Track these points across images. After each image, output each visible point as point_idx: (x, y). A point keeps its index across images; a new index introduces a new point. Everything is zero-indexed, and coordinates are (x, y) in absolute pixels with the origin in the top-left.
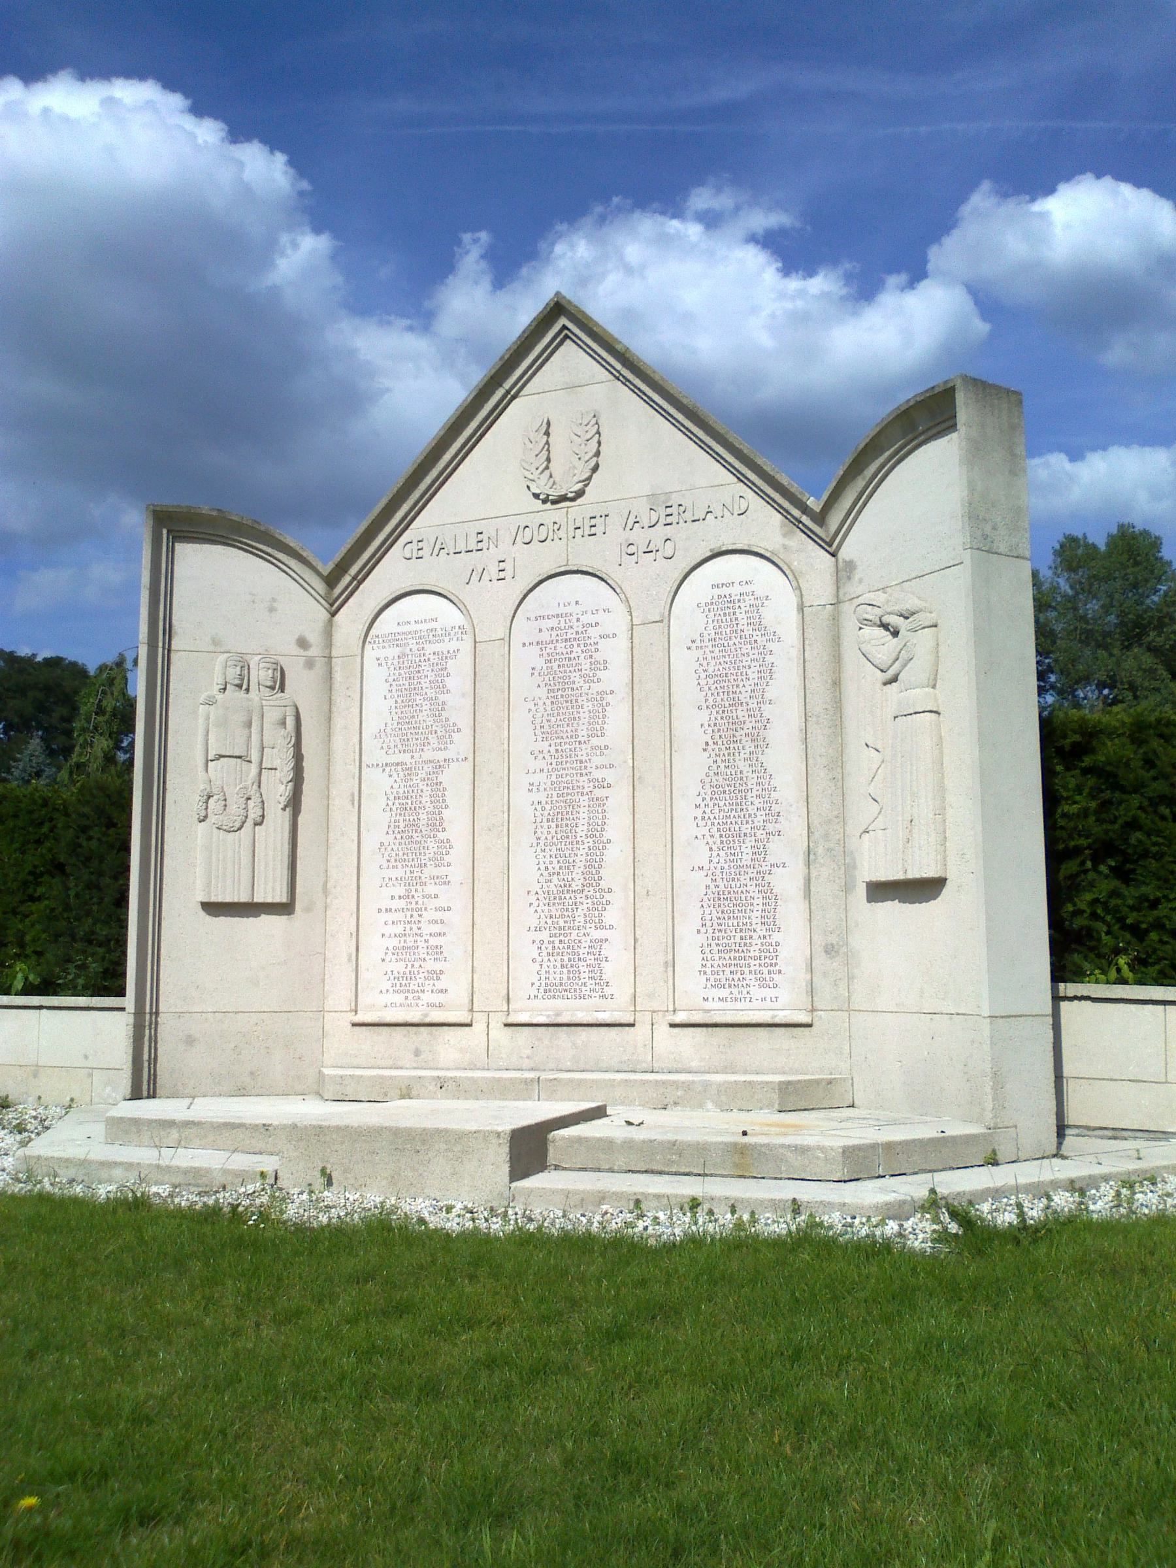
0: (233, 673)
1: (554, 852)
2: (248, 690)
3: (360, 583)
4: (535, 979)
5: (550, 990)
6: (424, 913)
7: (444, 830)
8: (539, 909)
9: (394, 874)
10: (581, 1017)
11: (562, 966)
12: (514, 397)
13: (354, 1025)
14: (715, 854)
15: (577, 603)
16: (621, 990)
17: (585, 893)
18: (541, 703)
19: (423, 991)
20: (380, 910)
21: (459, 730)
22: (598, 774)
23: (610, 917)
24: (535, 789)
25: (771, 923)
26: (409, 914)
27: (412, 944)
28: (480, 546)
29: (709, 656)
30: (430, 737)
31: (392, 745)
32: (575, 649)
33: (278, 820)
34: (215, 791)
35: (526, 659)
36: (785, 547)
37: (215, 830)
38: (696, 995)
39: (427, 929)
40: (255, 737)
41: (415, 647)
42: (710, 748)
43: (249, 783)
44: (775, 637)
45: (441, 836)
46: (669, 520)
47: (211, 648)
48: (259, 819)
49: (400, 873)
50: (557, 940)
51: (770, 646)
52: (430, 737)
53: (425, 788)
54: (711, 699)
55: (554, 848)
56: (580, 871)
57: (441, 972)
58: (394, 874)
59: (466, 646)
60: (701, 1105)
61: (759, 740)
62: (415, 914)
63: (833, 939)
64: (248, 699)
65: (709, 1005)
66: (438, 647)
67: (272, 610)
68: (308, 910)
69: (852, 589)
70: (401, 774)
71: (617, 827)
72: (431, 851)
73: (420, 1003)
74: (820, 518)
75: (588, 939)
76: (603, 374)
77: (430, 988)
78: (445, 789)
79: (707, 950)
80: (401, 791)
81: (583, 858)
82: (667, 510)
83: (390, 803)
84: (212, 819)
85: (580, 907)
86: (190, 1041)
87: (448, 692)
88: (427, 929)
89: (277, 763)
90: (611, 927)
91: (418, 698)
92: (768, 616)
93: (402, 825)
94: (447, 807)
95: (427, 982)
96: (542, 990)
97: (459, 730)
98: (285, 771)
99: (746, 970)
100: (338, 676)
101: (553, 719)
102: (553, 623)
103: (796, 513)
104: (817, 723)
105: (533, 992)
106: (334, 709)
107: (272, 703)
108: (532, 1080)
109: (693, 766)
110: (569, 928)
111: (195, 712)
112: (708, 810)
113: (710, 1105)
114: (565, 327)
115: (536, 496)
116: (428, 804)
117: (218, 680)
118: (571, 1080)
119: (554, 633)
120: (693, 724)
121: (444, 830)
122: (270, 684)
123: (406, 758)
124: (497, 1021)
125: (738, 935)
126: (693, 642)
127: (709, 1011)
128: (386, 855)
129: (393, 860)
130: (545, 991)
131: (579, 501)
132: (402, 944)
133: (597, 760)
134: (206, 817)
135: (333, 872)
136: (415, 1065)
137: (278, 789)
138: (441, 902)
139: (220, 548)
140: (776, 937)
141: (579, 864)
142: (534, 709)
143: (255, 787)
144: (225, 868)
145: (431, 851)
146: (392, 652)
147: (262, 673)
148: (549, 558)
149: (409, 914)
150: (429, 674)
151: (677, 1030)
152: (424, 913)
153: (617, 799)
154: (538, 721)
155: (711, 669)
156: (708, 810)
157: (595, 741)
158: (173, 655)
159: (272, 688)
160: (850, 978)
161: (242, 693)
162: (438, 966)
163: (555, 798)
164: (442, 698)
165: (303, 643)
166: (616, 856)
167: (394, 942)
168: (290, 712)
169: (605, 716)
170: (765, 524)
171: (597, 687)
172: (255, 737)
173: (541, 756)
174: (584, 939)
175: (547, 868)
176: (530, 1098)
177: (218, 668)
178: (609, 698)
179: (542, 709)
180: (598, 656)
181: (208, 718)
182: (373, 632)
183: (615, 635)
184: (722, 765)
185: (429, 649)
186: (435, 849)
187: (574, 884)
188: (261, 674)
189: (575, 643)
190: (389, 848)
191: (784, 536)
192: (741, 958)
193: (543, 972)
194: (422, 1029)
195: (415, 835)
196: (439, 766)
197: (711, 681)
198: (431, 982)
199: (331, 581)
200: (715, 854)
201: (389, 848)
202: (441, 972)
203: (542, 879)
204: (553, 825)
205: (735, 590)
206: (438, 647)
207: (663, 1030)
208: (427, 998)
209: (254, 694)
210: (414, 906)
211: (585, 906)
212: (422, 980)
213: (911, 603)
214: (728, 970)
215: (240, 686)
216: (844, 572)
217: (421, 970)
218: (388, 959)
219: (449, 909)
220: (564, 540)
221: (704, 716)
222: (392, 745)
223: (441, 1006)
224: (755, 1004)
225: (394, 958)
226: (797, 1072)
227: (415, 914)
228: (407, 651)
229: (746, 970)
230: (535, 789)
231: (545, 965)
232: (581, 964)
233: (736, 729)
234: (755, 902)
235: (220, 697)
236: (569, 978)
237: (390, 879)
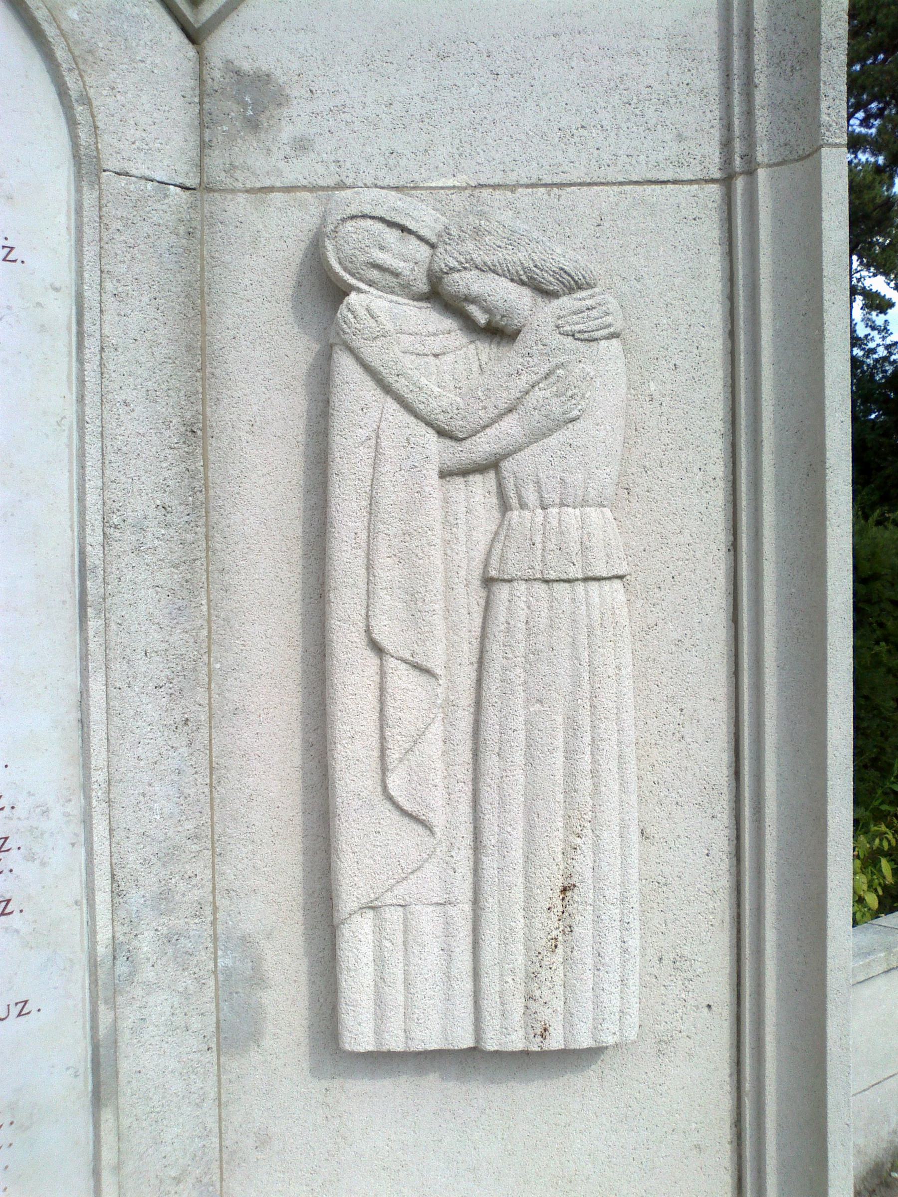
69: (261, 159)
104: (138, 549)
213: (563, 256)
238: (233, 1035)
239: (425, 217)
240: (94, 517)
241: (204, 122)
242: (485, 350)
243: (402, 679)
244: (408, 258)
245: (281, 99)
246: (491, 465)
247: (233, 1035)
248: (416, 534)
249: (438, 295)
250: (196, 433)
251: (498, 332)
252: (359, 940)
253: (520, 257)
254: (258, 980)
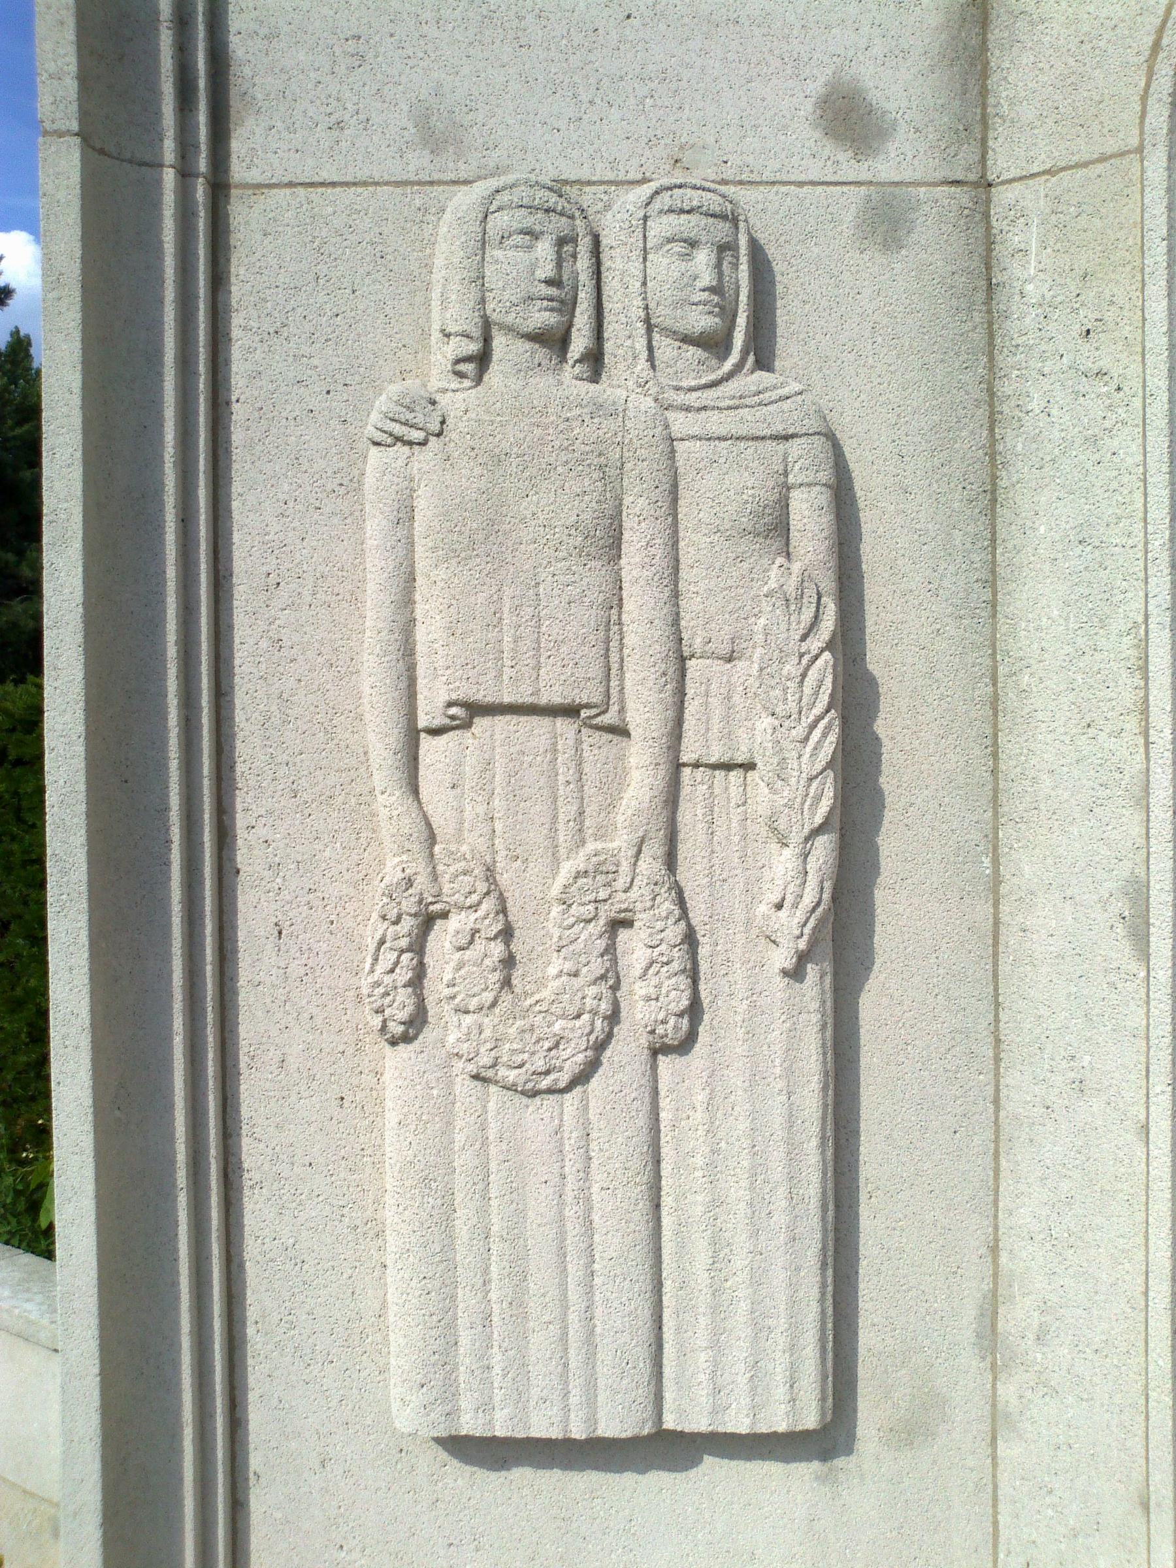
0: (519, 272)
2: (595, 360)
33: (766, 1021)
34: (452, 890)
37: (464, 1087)
40: (641, 606)
43: (621, 842)
47: (418, 163)
48: (674, 1029)
64: (598, 408)
68: (910, 1432)
84: (449, 1030)
89: (756, 735)
98: (794, 781)
100: (1030, 274)
106: (1014, 442)
107: (715, 423)
111: (355, 486)
117: (451, 311)
122: (701, 321)
134: (417, 1021)
135: (1023, 1257)
137: (764, 883)
143: (651, 865)
144: (520, 1276)
147: (664, 265)
158: (243, 216)
159: (715, 344)
161: (570, 381)
165: (848, 118)
168: (805, 461)
172: (641, 606)
177: (448, 250)
181: (405, 515)
188: (653, 278)
209: (624, 379)
215: (555, 341)
235: (459, 401)
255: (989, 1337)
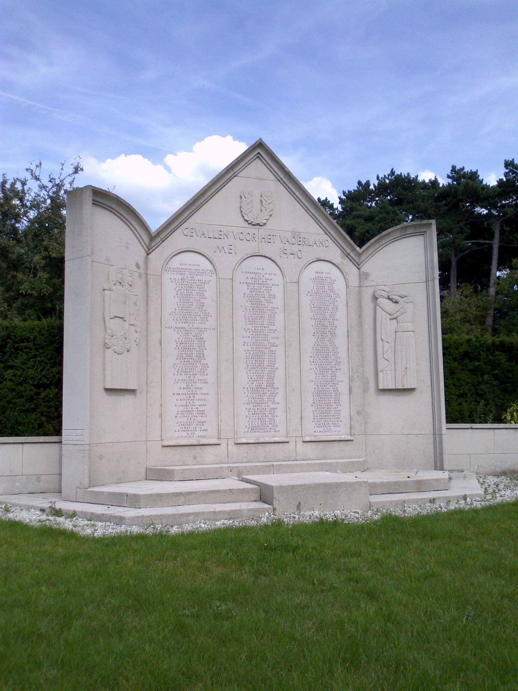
1: (254, 371)
3: (163, 242)
4: (247, 424)
5: (253, 429)
6: (196, 396)
7: (205, 359)
8: (248, 395)
9: (181, 378)
10: (267, 440)
11: (259, 419)
12: (235, 176)
13: (163, 446)
14: (318, 376)
15: (263, 269)
16: (282, 429)
17: (268, 389)
18: (248, 309)
19: (196, 431)
20: (174, 394)
21: (211, 316)
22: (273, 341)
23: (279, 398)
24: (246, 345)
25: (338, 402)
26: (188, 396)
27: (190, 409)
28: (220, 237)
29: (315, 299)
30: (197, 317)
31: (178, 319)
32: (262, 288)
35: (241, 290)
36: (342, 263)
38: (311, 430)
39: (197, 403)
41: (189, 276)
42: (315, 335)
44: (338, 296)
45: (203, 362)
46: (300, 243)
49: (183, 377)
50: (256, 408)
51: (337, 299)
52: (197, 317)
53: (195, 340)
54: (315, 316)
55: (254, 370)
56: (265, 380)
57: (205, 422)
58: (181, 378)
59: (213, 279)
60: (335, 472)
61: (333, 334)
62: (191, 396)
63: (360, 409)
65: (315, 434)
66: (200, 278)
67: (127, 248)
69: (367, 283)
70: (184, 333)
71: (280, 363)
72: (199, 368)
73: (195, 436)
74: (360, 255)
75: (269, 408)
76: (272, 177)
77: (199, 429)
78: (204, 341)
79: (315, 413)
80: (183, 340)
81: (267, 375)
82: (298, 238)
83: (178, 345)
85: (266, 395)
86: (101, 457)
87: (206, 298)
88: (197, 403)
90: (278, 403)
91: (191, 299)
92: (335, 287)
93: (184, 356)
94: (206, 349)
95: (198, 426)
96: (250, 429)
97: (211, 316)
99: (329, 420)
100: (151, 283)
101: (254, 316)
102: (253, 275)
103: (349, 251)
105: (246, 430)
106: (149, 299)
108: (270, 466)
109: (309, 341)
110: (261, 403)
112: (315, 359)
113: (339, 471)
114: (259, 153)
115: (247, 221)
116: (197, 348)
118: (286, 465)
119: (253, 280)
120: (309, 325)
121: (205, 359)
123: (186, 325)
124: (231, 443)
125: (326, 407)
126: (309, 293)
127: (316, 436)
128: (177, 369)
129: (180, 371)
130: (252, 429)
131: (263, 227)
132: (185, 409)
133: (272, 335)
136: (193, 463)
138: (203, 391)
139: (108, 213)
140: (340, 408)
141: (264, 377)
142: (245, 311)
145: (199, 368)
146: (178, 277)
148: (251, 248)
149: (188, 396)
150: (196, 289)
151: (305, 444)
152: (196, 396)
153: (280, 351)
154: (247, 316)
155: (315, 305)
156: (315, 359)
157: (271, 327)
160: (366, 423)
162: (203, 419)
163: (254, 349)
164: (202, 300)
166: (279, 374)
167: (182, 408)
169: (275, 318)
170: (334, 252)
171: (271, 305)
173: (248, 331)
174: (267, 408)
175: (251, 378)
176: (270, 473)
178: (276, 310)
179: (248, 311)
180: (271, 292)
182: (168, 266)
183: (278, 285)
184: (320, 342)
185: (196, 278)
186: (201, 367)
187: (263, 385)
189: (262, 286)
190: (178, 366)
191: (342, 258)
192: (327, 416)
193: (251, 421)
194: (197, 447)
195: (191, 361)
196: (201, 331)
197: (315, 309)
198: (200, 426)
199: (152, 238)
200: (318, 376)
201: (178, 366)
202: (205, 422)
203: (250, 383)
204: (254, 360)
205: (324, 275)
206: (200, 278)
207: (300, 444)
208: (198, 433)
210: (191, 392)
211: (268, 395)
212: (195, 426)
213: (404, 293)
214: (323, 420)
216: (364, 276)
217: (195, 421)
218: (178, 416)
219: (208, 394)
220: (257, 242)
221: (313, 322)
222: (178, 319)
223: (204, 437)
224: (333, 433)
225: (181, 416)
226: (348, 458)
227: (191, 396)
228: (186, 278)
229: (329, 420)
230: (246, 345)
231: (251, 418)
232: (266, 418)
233: (324, 330)
234: (332, 395)
236: (261, 424)
237: (179, 380)
238: (365, 390)
239: (387, 289)
240: (349, 326)
241: (360, 279)
242: (395, 304)
243: (385, 344)
244: (385, 294)
245: (369, 275)
246: (396, 318)
247: (365, 390)
248: (386, 327)
249: (389, 298)
250: (360, 316)
251: (396, 302)
252: (381, 375)
253: (398, 294)
254: (368, 383)
255: (147, 384)
